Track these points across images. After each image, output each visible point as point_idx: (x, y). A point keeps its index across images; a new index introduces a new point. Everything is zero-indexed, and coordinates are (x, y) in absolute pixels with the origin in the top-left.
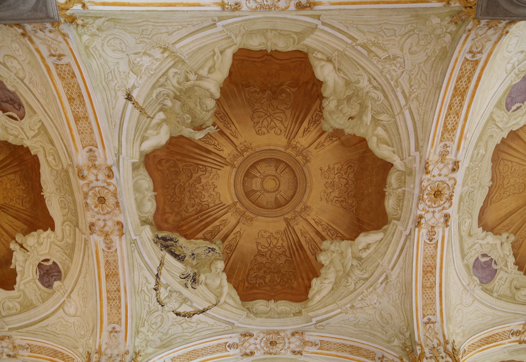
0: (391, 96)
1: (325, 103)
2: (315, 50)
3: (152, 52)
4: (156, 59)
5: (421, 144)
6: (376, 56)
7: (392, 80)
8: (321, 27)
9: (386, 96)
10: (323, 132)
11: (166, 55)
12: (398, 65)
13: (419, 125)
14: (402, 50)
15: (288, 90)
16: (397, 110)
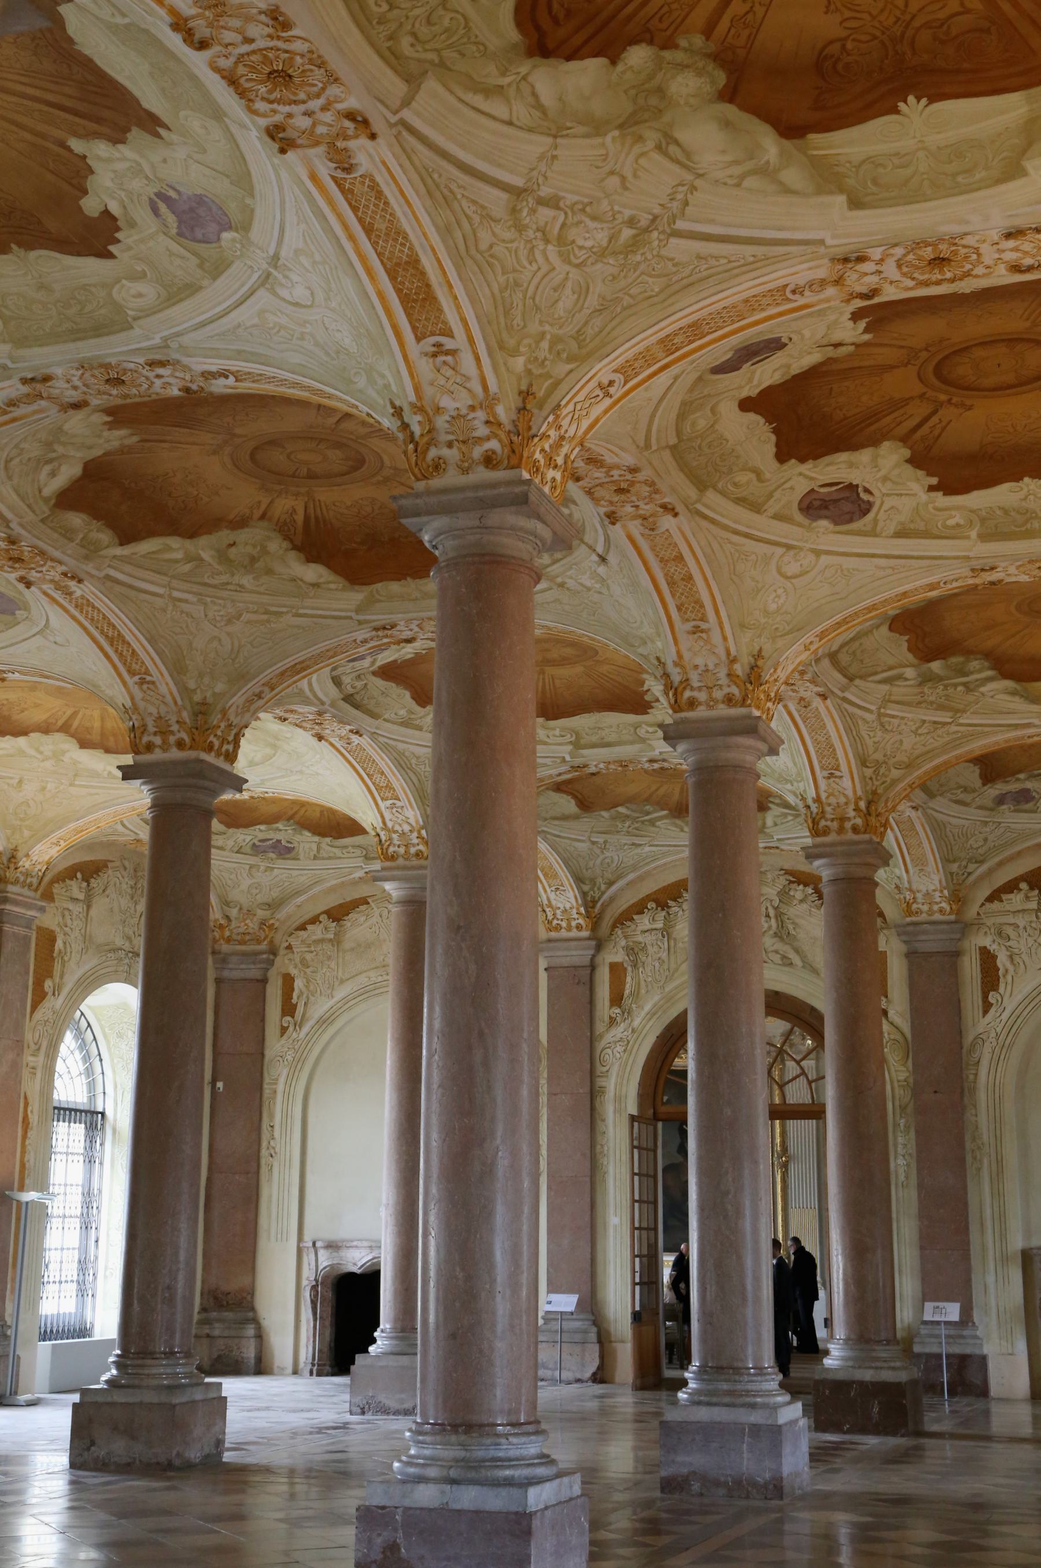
0: (196, 588)
1: (286, 544)
2: (343, 590)
3: (580, 588)
4: (571, 578)
5: (109, 584)
6: (255, 612)
7: (212, 602)
8: (353, 614)
9: (205, 584)
10: (263, 517)
11: (559, 580)
12: (218, 618)
13: (133, 594)
14: (229, 634)
15: (354, 545)
16: (175, 583)
